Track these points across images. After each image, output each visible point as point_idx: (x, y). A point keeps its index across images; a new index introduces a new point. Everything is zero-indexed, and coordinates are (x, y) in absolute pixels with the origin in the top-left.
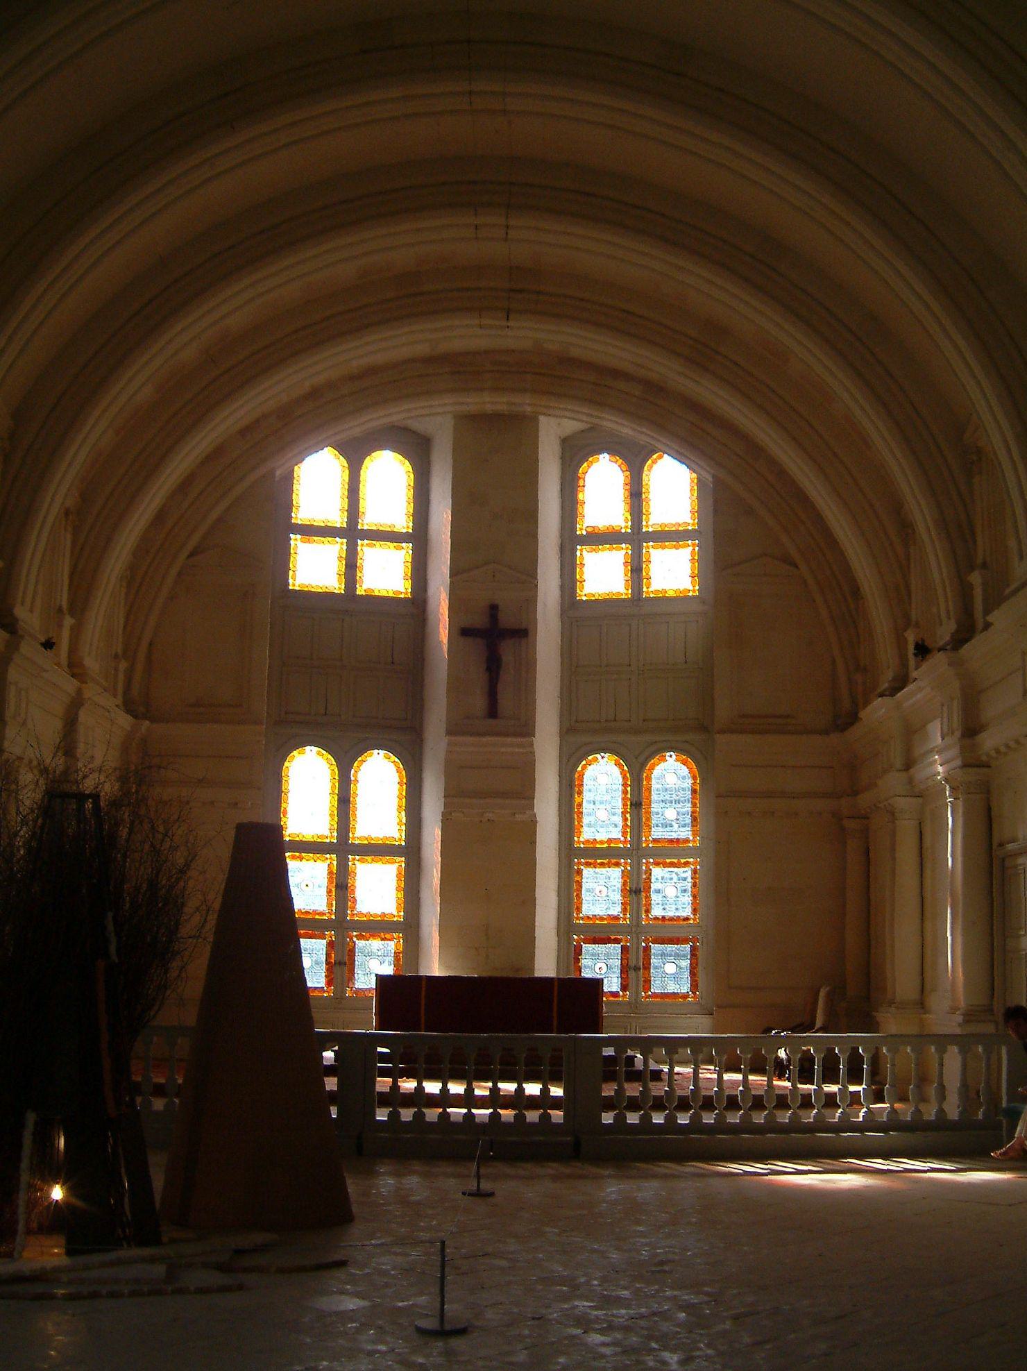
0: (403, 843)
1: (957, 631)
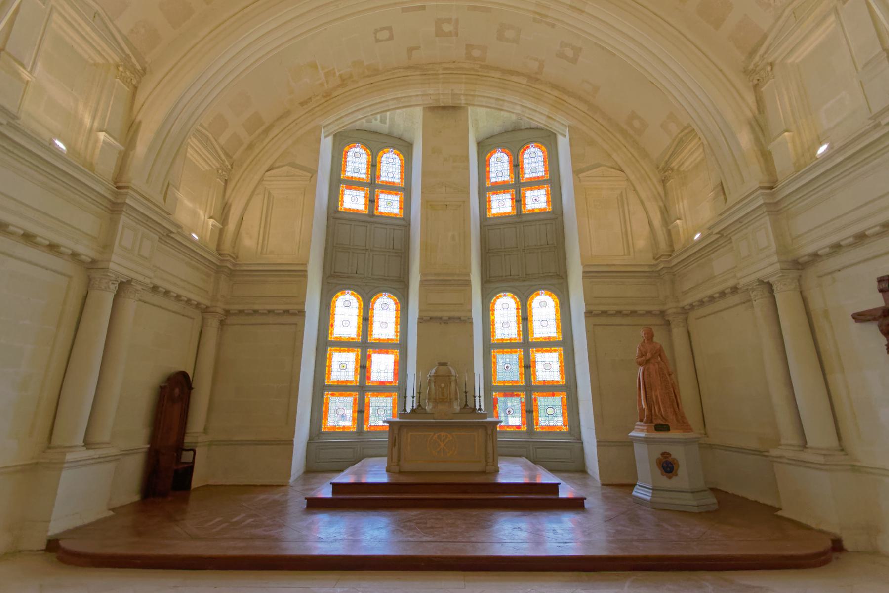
0: (398, 342)
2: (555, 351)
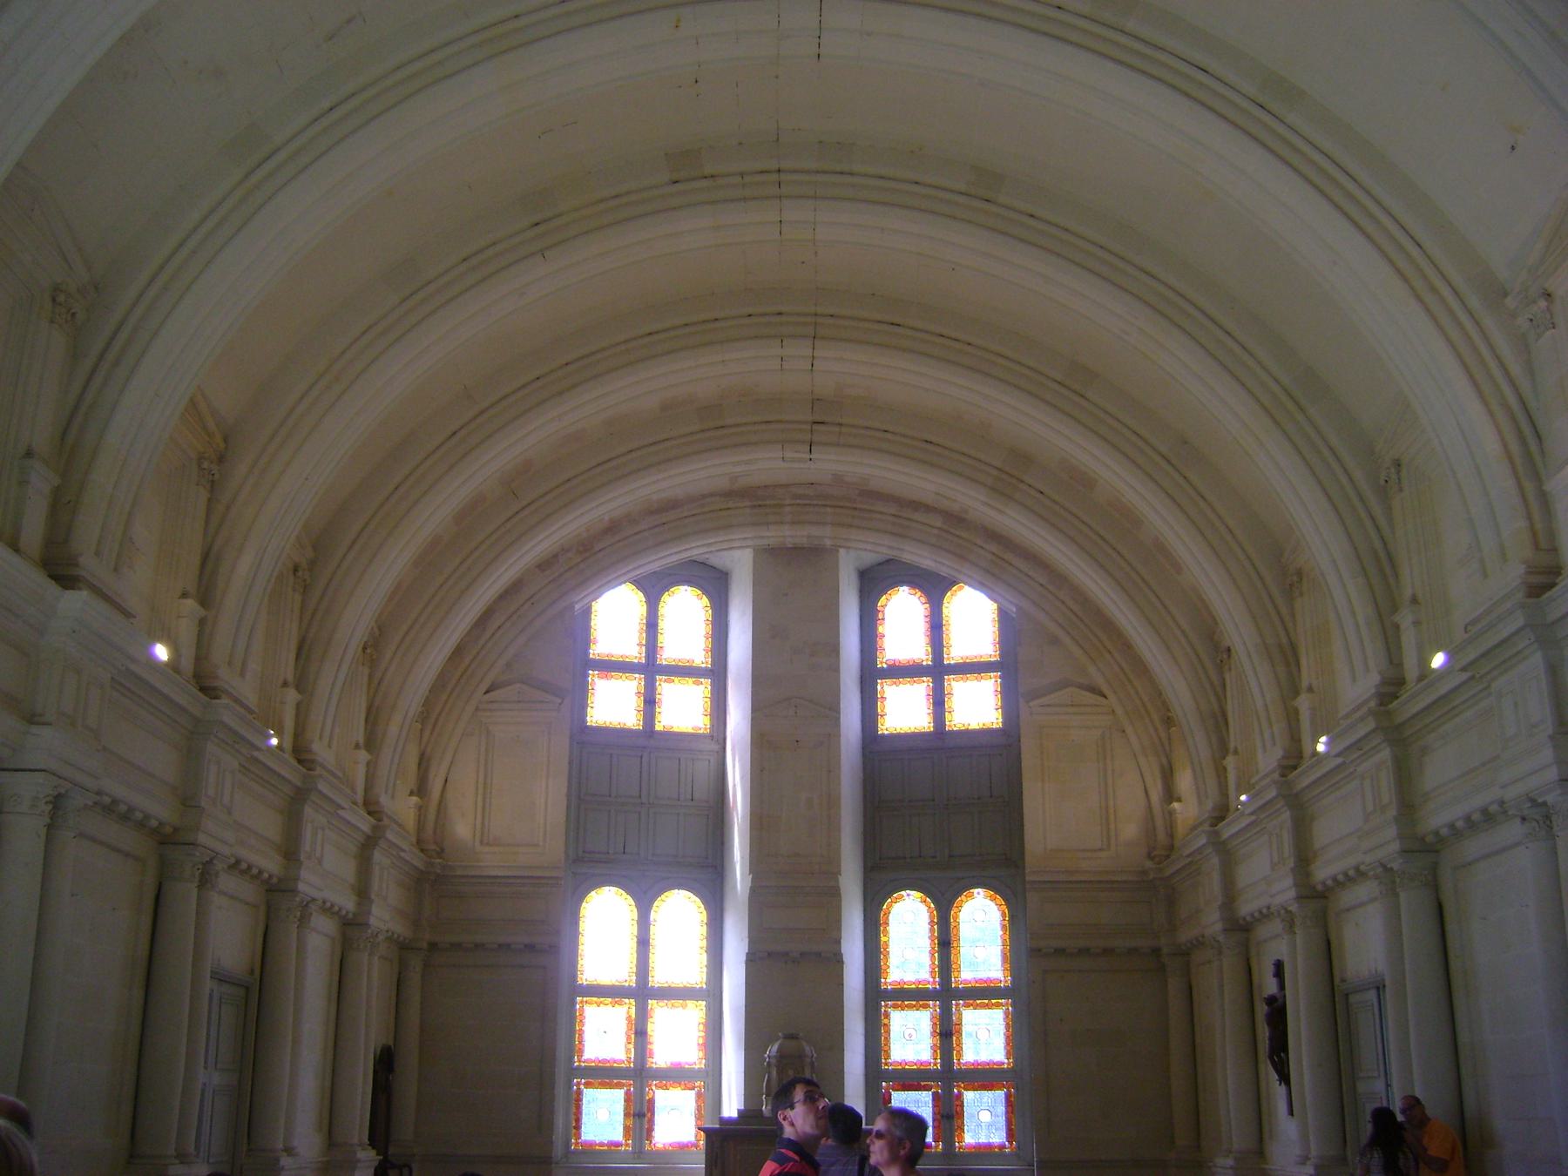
1: (1284, 757)
2: (998, 1006)
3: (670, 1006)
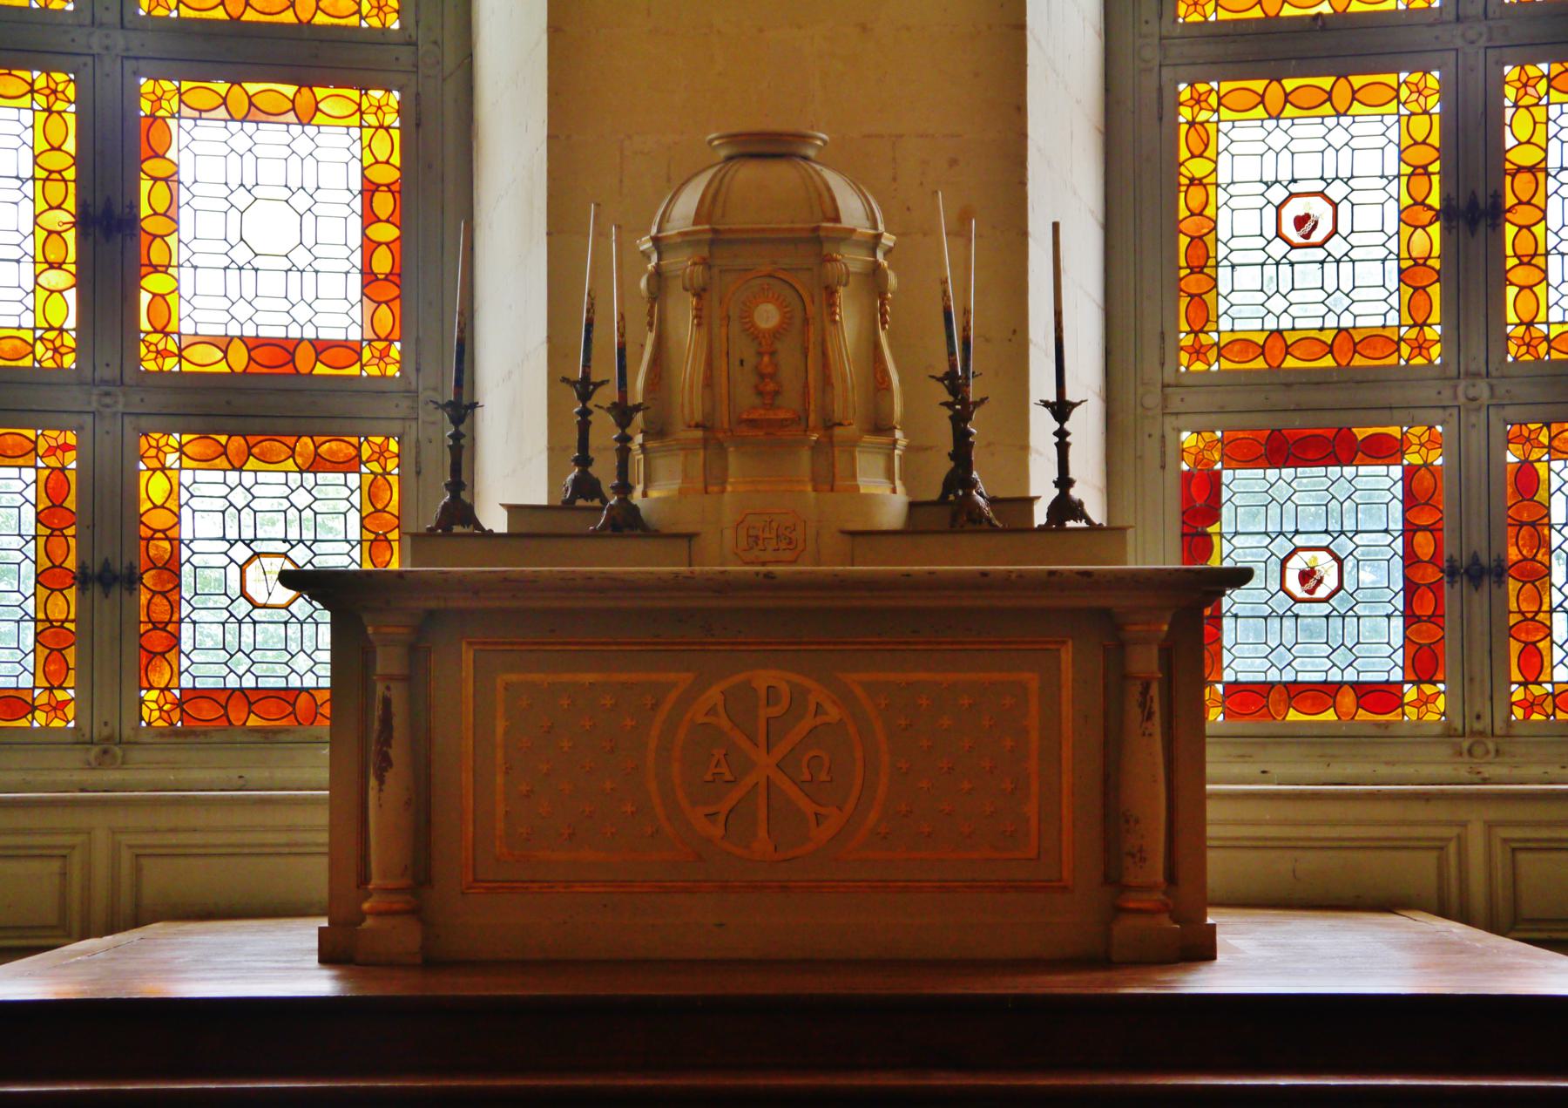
3: (240, 107)
